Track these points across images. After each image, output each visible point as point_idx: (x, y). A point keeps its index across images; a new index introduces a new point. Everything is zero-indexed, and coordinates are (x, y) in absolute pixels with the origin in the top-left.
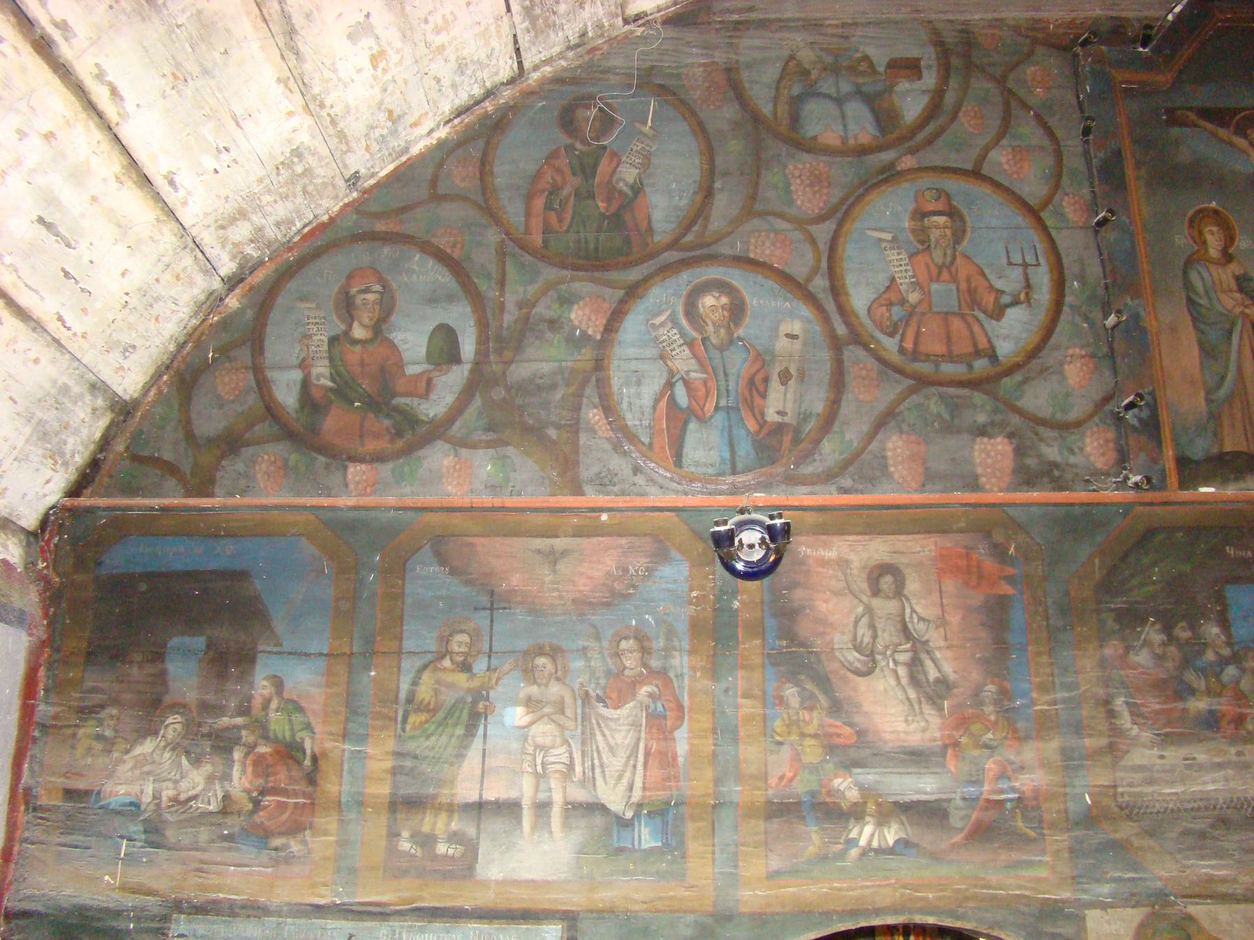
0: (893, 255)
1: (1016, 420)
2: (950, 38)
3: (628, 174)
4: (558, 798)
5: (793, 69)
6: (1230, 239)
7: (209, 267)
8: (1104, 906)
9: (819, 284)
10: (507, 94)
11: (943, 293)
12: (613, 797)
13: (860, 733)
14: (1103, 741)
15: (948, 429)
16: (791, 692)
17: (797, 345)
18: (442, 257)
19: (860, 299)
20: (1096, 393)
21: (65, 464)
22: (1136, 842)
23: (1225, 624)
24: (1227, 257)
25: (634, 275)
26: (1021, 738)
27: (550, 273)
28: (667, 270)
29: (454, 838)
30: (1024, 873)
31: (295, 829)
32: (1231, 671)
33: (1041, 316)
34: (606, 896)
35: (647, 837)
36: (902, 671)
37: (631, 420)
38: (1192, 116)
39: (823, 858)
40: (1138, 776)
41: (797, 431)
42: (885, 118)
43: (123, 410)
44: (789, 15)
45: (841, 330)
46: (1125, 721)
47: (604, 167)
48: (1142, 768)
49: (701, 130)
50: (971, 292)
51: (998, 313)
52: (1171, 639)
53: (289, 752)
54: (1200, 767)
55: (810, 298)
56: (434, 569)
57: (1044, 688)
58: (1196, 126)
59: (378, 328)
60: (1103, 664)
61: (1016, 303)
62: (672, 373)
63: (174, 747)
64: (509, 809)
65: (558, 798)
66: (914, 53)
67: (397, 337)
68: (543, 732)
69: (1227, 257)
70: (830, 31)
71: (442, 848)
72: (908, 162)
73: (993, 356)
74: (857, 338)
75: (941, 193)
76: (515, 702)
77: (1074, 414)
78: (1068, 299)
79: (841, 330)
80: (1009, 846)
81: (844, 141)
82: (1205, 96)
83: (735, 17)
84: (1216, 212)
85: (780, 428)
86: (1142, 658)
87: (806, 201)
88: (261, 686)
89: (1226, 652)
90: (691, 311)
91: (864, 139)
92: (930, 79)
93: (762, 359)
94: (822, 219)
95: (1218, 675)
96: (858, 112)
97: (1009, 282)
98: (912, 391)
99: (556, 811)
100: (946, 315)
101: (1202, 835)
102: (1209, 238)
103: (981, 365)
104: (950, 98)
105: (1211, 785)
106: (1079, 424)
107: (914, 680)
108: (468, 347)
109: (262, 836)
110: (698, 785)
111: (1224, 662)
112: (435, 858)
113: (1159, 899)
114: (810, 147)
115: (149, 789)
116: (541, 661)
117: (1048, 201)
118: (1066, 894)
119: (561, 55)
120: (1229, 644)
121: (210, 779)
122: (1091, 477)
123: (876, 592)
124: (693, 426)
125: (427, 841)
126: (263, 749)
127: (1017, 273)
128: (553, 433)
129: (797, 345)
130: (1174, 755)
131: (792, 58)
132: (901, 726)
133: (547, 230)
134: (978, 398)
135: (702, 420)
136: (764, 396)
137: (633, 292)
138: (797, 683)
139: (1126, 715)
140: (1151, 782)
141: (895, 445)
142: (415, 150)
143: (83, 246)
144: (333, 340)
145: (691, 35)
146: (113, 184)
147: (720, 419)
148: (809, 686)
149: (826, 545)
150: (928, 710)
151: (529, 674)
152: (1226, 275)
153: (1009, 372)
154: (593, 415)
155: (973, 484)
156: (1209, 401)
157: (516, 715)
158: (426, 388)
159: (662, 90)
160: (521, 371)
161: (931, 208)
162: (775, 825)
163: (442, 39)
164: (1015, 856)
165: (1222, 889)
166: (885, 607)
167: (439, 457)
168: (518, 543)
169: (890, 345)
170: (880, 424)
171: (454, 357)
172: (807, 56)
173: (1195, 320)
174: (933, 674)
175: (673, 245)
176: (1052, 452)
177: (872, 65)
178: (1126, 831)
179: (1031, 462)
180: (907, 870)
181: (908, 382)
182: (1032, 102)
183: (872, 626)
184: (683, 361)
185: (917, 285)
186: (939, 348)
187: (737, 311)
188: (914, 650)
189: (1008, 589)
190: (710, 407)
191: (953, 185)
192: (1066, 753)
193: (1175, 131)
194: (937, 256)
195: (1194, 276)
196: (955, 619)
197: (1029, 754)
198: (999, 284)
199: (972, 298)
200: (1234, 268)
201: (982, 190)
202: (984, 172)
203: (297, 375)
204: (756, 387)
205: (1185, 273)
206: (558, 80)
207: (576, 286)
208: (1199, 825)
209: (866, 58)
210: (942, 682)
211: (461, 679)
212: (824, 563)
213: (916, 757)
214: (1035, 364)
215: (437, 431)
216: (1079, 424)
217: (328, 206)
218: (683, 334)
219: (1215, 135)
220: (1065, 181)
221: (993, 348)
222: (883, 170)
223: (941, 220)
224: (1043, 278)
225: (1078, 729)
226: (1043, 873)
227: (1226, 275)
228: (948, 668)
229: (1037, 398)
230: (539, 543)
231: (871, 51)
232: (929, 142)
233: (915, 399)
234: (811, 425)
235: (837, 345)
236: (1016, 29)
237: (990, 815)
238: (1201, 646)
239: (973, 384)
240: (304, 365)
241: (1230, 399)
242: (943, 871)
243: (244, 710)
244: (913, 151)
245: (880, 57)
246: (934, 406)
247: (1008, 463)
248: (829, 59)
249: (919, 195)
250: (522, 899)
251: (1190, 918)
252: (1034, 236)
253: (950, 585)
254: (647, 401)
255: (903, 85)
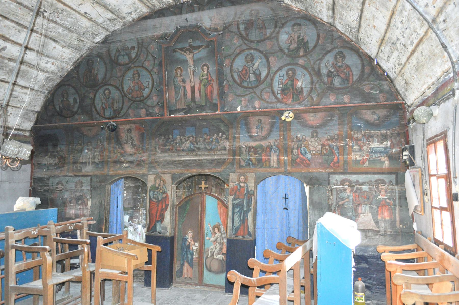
0: (130, 82)
1: (146, 106)
2: (140, 41)
3: (96, 72)
4: (91, 161)
5: (118, 51)
6: (182, 72)
7: (44, 93)
8: (151, 174)
9: (120, 87)
10: (80, 59)
11: (137, 87)
12: (96, 161)
13: (125, 152)
14: (154, 153)
15: (137, 108)
16: (117, 147)
17: (118, 97)
18: (73, 87)
19: (125, 89)
20: (157, 101)
21: (32, 121)
22: (156, 166)
23: (172, 136)
24: (181, 75)
25: (97, 88)
26: (144, 152)
27: (87, 89)
28: (101, 87)
29: (80, 167)
30: (142, 170)
31: (63, 167)
32: (172, 142)
33: (150, 89)
34: (95, 173)
35: (100, 166)
36: (131, 143)
37: (98, 110)
38: (177, 50)
39: (119, 168)
40: (158, 157)
41: (118, 110)
42: (130, 58)
43: (39, 113)
44: (118, 40)
45: (123, 94)
46: (157, 150)
47: (93, 71)
48: (158, 156)
49: (105, 63)
50: (140, 86)
51: (144, 90)
52: (165, 138)
53: (62, 157)
54: (166, 156)
55: (119, 90)
56: (77, 132)
57: (148, 145)
58: (178, 52)
59: (67, 99)
60: (156, 142)
61: (147, 88)
62: (103, 103)
63: (50, 157)
64: (85, 163)
65: (91, 161)
66: (134, 45)
67: (69, 100)
68: (89, 153)
69: (181, 75)
70: (123, 42)
71: (78, 168)
72: (133, 65)
73: (143, 97)
74: (125, 96)
75: (137, 70)
76: (86, 149)
77: (154, 105)
78: (154, 86)
79: (123, 94)
80: (141, 167)
81: (124, 63)
82: (180, 46)
83: (110, 41)
84: (180, 68)
85: (116, 110)
86: (161, 141)
87: (119, 74)
88: (59, 149)
89: (172, 140)
90: (104, 93)
91: (127, 62)
92: (136, 50)
93: (113, 99)
94: (121, 76)
95: (170, 143)
96: (126, 57)
97: (145, 84)
98: (133, 103)
99: (91, 163)
100: (137, 91)
101: (165, 165)
102: (178, 72)
103: (142, 98)
104: (139, 53)
105: (167, 159)
106: (155, 106)
107: (132, 144)
108: (78, 101)
109: (59, 168)
110: (105, 159)
111: (172, 141)
112: (78, 169)
113: (158, 174)
114: (120, 65)
115: (47, 162)
116: (89, 144)
117: (152, 70)
118: (146, 173)
119: (87, 51)
120: (173, 138)
121: (53, 161)
122: (157, 114)
123: (128, 132)
124: (106, 110)
125: (77, 167)
126: (59, 157)
127: (147, 83)
128: (89, 112)
129: (118, 97)
130: (163, 154)
131: (117, 48)
132: (130, 151)
133: (86, 82)
134: (141, 103)
135: (107, 109)
136: (114, 105)
137: (97, 91)
138: (118, 145)
139: (158, 149)
140: (159, 158)
141: (130, 111)
142: (69, 70)
143: (20, 97)
144: (62, 101)
145: (104, 45)
146: (21, 90)
147: (109, 109)
148: (119, 146)
149: (122, 126)
150: (133, 149)
151: (88, 145)
152: (180, 79)
153: (146, 99)
154: (94, 109)
155: (141, 117)
156: (175, 101)
157: (86, 151)
158: (74, 107)
159: (100, 57)
160: (85, 104)
161: (135, 73)
162: (114, 164)
163: (63, 58)
164: (141, 168)
165: (166, 172)
166: (129, 135)
167: (77, 117)
168: (86, 128)
169: (130, 96)
170: (129, 108)
171: (76, 102)
172: (119, 47)
173: (175, 87)
174: (134, 143)
175: (102, 83)
176: (151, 111)
177: (128, 48)
178: (155, 165)
179: (148, 113)
180: (129, 170)
181: (132, 102)
182: (151, 52)
183: (127, 137)
184: (104, 101)
185: (133, 86)
186: (136, 96)
187: (110, 93)
188: (132, 140)
189: (144, 131)
190: (107, 107)
191: (139, 69)
192: (149, 154)
193: (175, 53)
194: (136, 81)
195: (175, 79)
196: (137, 136)
197: (145, 154)
198: (144, 85)
199: (140, 88)
200: (182, 77)
201: (142, 69)
202: (143, 66)
203: (58, 106)
204: (113, 104)
205: (174, 79)
206: (87, 56)
207: (90, 91)
208: (164, 164)
209: (128, 47)
210: (135, 145)
211: (80, 146)
212: (122, 129)
213: (131, 155)
214: (149, 97)
215: (76, 113)
216: (155, 106)
217: (58, 81)
218: (104, 97)
219: (181, 53)
220: (155, 66)
221: (143, 95)
222: (129, 67)
223: (136, 75)
224: (151, 83)
225: (151, 151)
226: (144, 170)
227: (180, 79)
228: (136, 143)
229: (149, 103)
230: (89, 128)
231: (128, 45)
232: (135, 62)
233: (133, 104)
234: (120, 109)
235: (123, 97)
236: (150, 38)
237: (139, 163)
238: (169, 139)
239: (140, 101)
240: (59, 104)
241: (179, 100)
242: (132, 170)
243: (57, 152)
244: (133, 64)
245: (129, 46)
246: (135, 105)
247: (145, 113)
248: (122, 48)
249: (134, 71)
250: (86, 174)
251: (161, 176)
252: (150, 76)
253: (137, 131)
254: (100, 107)
255: (133, 52)
